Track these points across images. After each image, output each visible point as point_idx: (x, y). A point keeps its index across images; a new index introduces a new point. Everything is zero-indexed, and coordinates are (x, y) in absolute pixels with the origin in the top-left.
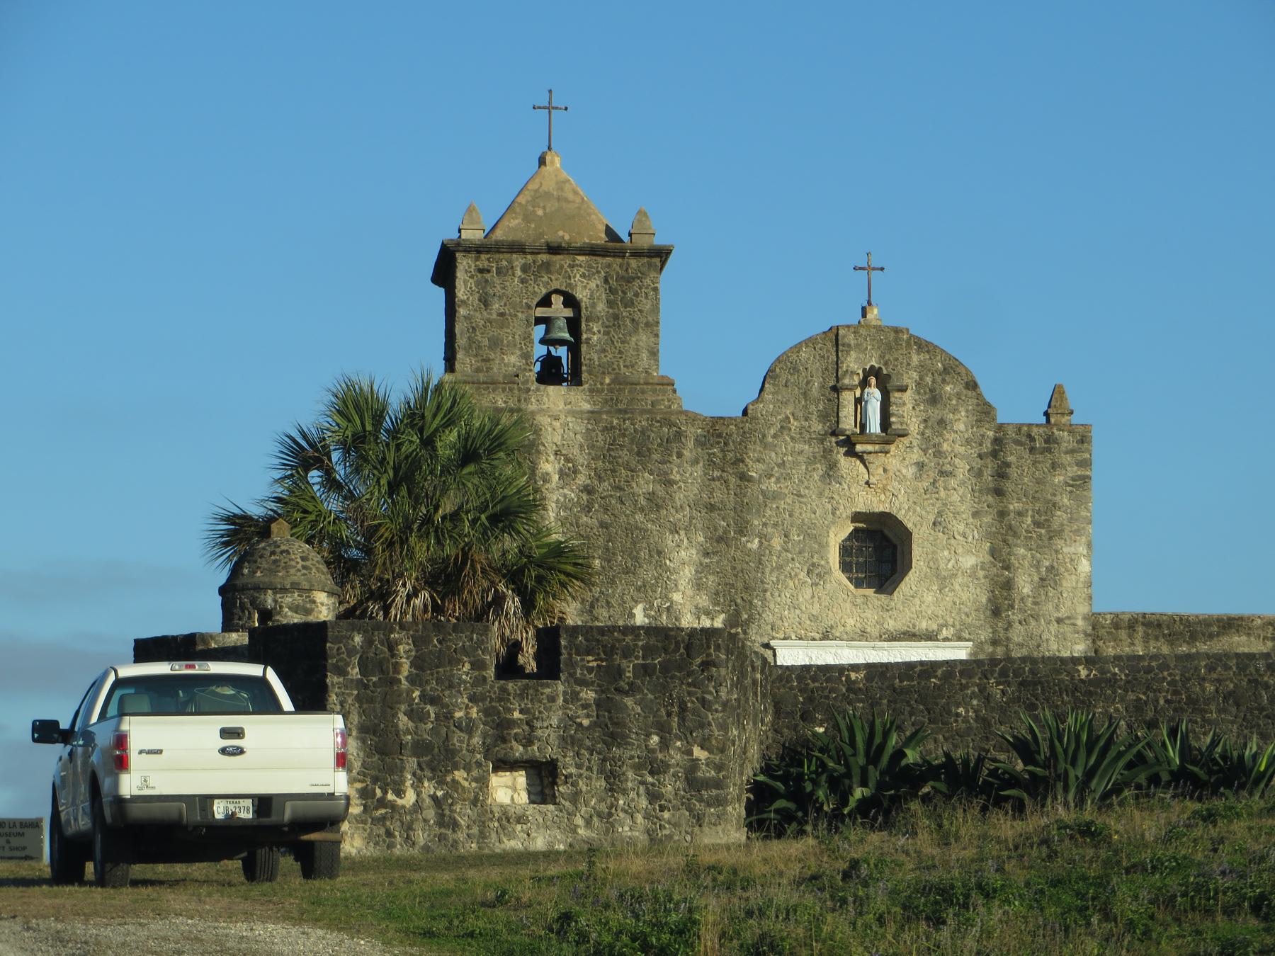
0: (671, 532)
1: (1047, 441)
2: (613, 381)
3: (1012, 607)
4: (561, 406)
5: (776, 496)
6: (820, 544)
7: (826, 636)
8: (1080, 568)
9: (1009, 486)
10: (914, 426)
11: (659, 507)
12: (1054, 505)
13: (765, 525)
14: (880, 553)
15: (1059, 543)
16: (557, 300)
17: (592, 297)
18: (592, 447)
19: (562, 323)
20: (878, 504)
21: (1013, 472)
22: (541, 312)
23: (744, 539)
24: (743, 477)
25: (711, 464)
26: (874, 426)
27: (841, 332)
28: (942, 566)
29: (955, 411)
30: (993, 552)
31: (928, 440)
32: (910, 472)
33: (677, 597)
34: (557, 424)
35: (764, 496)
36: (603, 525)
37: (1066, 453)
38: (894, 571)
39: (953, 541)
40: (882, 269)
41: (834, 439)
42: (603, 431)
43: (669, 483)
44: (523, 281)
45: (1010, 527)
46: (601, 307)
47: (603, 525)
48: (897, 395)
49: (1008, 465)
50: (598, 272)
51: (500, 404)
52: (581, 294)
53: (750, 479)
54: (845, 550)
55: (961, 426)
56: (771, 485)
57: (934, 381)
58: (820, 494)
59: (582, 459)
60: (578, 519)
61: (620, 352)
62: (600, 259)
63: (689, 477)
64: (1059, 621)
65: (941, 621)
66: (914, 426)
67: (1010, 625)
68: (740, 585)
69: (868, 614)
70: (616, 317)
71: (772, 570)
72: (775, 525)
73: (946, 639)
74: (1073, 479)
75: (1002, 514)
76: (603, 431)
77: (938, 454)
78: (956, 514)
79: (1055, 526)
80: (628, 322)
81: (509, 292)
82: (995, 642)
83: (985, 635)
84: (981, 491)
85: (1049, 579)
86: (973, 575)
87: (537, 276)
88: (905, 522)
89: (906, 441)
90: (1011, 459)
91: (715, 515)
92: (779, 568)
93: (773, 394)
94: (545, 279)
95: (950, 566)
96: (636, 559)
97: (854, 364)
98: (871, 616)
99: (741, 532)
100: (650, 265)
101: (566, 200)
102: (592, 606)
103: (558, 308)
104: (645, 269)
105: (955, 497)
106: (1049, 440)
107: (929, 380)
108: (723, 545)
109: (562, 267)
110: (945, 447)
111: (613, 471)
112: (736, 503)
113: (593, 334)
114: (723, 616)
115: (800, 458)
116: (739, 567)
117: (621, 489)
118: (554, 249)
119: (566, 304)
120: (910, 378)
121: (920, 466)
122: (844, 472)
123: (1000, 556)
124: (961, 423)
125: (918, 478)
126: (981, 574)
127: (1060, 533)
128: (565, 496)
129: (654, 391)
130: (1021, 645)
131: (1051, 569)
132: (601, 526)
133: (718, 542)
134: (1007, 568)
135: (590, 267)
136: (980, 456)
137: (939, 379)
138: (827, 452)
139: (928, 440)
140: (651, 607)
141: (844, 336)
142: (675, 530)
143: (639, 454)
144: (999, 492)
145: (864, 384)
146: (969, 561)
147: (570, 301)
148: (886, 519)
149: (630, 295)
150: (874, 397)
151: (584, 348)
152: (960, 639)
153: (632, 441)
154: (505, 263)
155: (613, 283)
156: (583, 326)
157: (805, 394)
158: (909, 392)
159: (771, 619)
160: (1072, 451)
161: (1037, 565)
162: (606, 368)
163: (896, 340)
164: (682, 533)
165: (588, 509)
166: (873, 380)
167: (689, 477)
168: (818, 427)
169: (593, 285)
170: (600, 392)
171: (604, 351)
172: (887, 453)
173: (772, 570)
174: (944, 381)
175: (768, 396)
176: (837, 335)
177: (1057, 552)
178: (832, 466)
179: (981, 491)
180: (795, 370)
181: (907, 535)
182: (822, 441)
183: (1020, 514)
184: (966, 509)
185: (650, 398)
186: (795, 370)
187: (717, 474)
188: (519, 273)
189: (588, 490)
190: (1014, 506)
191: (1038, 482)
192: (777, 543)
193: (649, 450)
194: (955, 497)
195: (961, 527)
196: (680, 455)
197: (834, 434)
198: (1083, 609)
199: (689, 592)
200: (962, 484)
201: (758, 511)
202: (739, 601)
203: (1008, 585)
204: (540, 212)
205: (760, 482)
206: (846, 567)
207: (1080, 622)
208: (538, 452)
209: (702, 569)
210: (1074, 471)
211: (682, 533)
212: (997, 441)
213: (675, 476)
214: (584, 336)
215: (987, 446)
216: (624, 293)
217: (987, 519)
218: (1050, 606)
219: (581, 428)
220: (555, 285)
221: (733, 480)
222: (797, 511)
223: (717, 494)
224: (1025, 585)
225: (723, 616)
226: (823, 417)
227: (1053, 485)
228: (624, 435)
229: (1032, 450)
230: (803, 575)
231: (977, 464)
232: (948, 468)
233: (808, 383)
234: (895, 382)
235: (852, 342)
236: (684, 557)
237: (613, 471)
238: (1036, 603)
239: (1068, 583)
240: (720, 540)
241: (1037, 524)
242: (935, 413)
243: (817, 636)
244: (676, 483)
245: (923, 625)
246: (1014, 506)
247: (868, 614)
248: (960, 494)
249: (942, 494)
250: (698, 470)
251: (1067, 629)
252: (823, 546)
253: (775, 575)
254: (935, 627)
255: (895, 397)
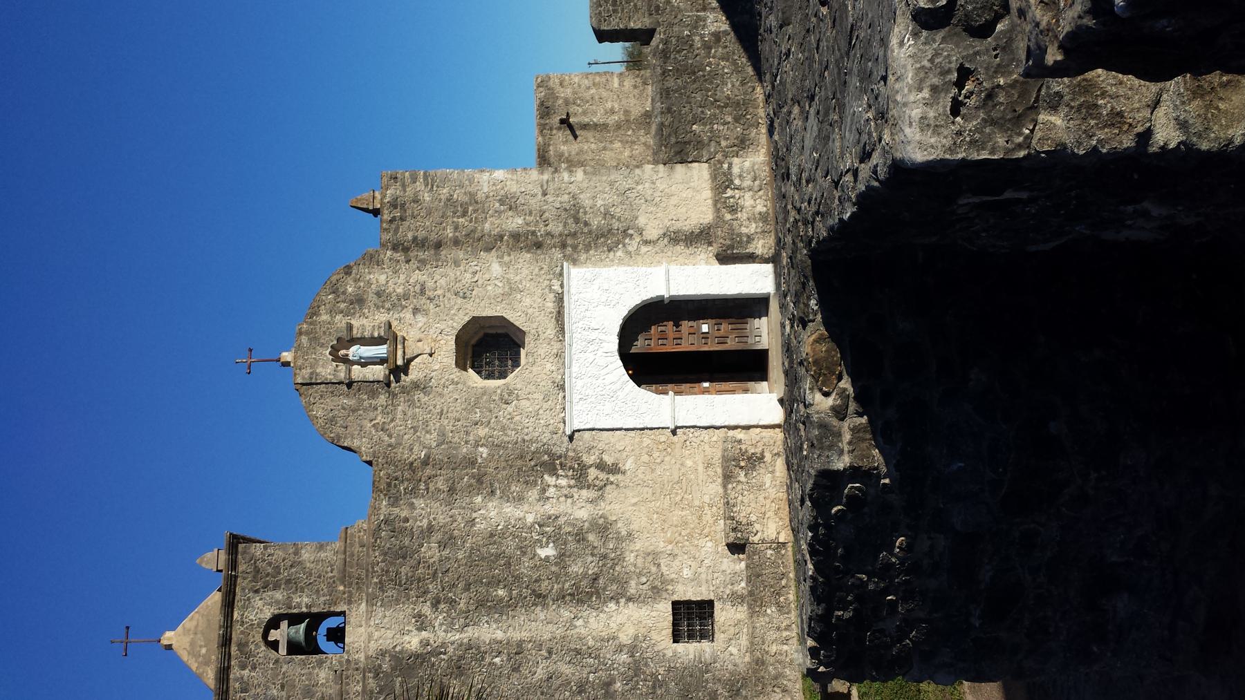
0: (474, 525)
1: (395, 207)
2: (343, 583)
3: (534, 233)
4: (362, 630)
5: (442, 434)
6: (483, 394)
7: (562, 387)
8: (501, 178)
9: (433, 237)
10: (382, 317)
11: (452, 537)
12: (449, 200)
13: (466, 442)
14: (490, 346)
15: (480, 196)
16: (274, 635)
17: (271, 604)
18: (397, 601)
19: (293, 630)
20: (448, 348)
21: (421, 234)
22: (283, 650)
23: (479, 460)
24: (425, 463)
25: (413, 492)
26: (381, 350)
27: (299, 380)
28: (500, 291)
29: (369, 283)
30: (488, 249)
31: (394, 306)
32: (421, 319)
33: (530, 519)
34: (377, 634)
35: (442, 443)
36: (467, 588)
37: (405, 191)
38: (506, 335)
39: (480, 283)
40: (251, 350)
41: (393, 385)
42: (383, 591)
43: (430, 529)
44: (254, 668)
45: (467, 235)
46: (279, 595)
47: (467, 588)
48: (355, 332)
49: (415, 238)
50: (249, 599)
51: (359, 688)
52: (267, 614)
53: (428, 457)
54: (490, 376)
55: (383, 278)
56: (431, 439)
57: (344, 302)
58: (441, 395)
59: (408, 609)
60: (462, 612)
61: (319, 577)
62: (237, 598)
63: (424, 511)
64: (545, 194)
65: (547, 290)
66: (382, 317)
67: (548, 234)
68: (519, 463)
69: (542, 351)
70: (288, 582)
71: (506, 435)
72: (467, 433)
73: (562, 286)
74: (427, 185)
75: (456, 242)
76: (383, 591)
77: (406, 296)
78: (457, 281)
79: (466, 199)
80: (293, 570)
81: (263, 680)
82: (564, 246)
83: (557, 254)
84: (437, 260)
85: (510, 203)
86: (508, 265)
87: (249, 655)
88: (464, 322)
89: (394, 324)
90: (410, 236)
91: (458, 487)
92: (503, 429)
93: (353, 438)
94: (252, 647)
95: (500, 285)
96: (498, 556)
97: (329, 370)
98: (543, 350)
99: (472, 463)
100: (244, 552)
101: (197, 626)
102: (539, 596)
103: (280, 634)
104: (248, 557)
105: (443, 282)
106: (394, 205)
107: (343, 306)
108: (486, 479)
109: (242, 632)
110: (400, 290)
111: (419, 580)
112: (448, 468)
113: (302, 602)
114: (546, 477)
115: (410, 413)
116: (504, 464)
117: (436, 572)
118: (226, 641)
119: (277, 627)
120: (340, 321)
121: (416, 311)
122: (421, 375)
123: (491, 243)
124: (379, 277)
125: (426, 312)
126: (506, 258)
127: (472, 195)
128: (441, 625)
129: (352, 545)
130: (565, 224)
131: (502, 202)
132: (468, 589)
133: (482, 483)
134: (501, 237)
135: (243, 607)
136: (408, 261)
137: (342, 297)
138: (404, 390)
139: (394, 306)
140: (539, 541)
141: (303, 378)
142: (472, 522)
143: (404, 558)
144: (438, 245)
145: (345, 360)
146: (496, 269)
147: (274, 623)
148: (460, 339)
149: (270, 570)
150: (355, 351)
151: (315, 610)
152: (561, 274)
153: (392, 564)
154: (237, 685)
155: (259, 585)
156: (295, 611)
157: (354, 411)
158: (353, 322)
159: (547, 435)
160: (404, 186)
161: (499, 212)
162: (332, 586)
163: (307, 333)
164: (474, 515)
165: (452, 603)
166: (342, 352)
167: (424, 511)
168: (382, 399)
169: (260, 603)
170: (351, 596)
171: (318, 591)
172: (404, 339)
173: (506, 435)
174: (344, 293)
175: (355, 444)
176: (303, 384)
177: (487, 197)
178: (416, 385)
179: (437, 260)
180: (332, 421)
181: (475, 320)
182: (394, 395)
183: (456, 228)
184: (451, 272)
185: (357, 549)
186: (332, 421)
187: (422, 486)
188: (246, 672)
189: (436, 604)
190: (450, 232)
191: (429, 213)
192: (482, 432)
193: (401, 548)
194: (443, 282)
195: (468, 276)
196: (406, 520)
197: (388, 385)
198: (534, 174)
199: (526, 507)
200: (431, 276)
201: (455, 448)
202: (533, 463)
203: (516, 236)
204: (204, 651)
205: (430, 448)
206: (503, 376)
207: (546, 177)
208: (401, 652)
209: (506, 497)
210: (420, 185)
211: (474, 515)
212: (395, 248)
213: (425, 523)
214: (304, 610)
215: (399, 256)
216: (268, 575)
217: (461, 254)
218: (532, 201)
219: (380, 611)
220: (259, 638)
221: (429, 471)
222: (455, 414)
223: (440, 485)
224: (515, 223)
225: (546, 477)
226: (373, 394)
227: (432, 201)
228: (387, 572)
229: (402, 219)
230: (510, 408)
231: (414, 264)
232: (418, 288)
233: (344, 408)
234: (344, 334)
235: (309, 371)
236: (494, 513)
237: (419, 580)
238: (531, 213)
239: (513, 188)
240: (480, 481)
241: (464, 214)
242: (371, 298)
243: (561, 394)
244: (430, 523)
245: (550, 305)
246: (450, 232)
247: (542, 351)
248: (440, 278)
249: (439, 292)
250: (419, 503)
251: (551, 190)
252: (485, 392)
253: (509, 432)
254: (552, 295)
255: (356, 333)
